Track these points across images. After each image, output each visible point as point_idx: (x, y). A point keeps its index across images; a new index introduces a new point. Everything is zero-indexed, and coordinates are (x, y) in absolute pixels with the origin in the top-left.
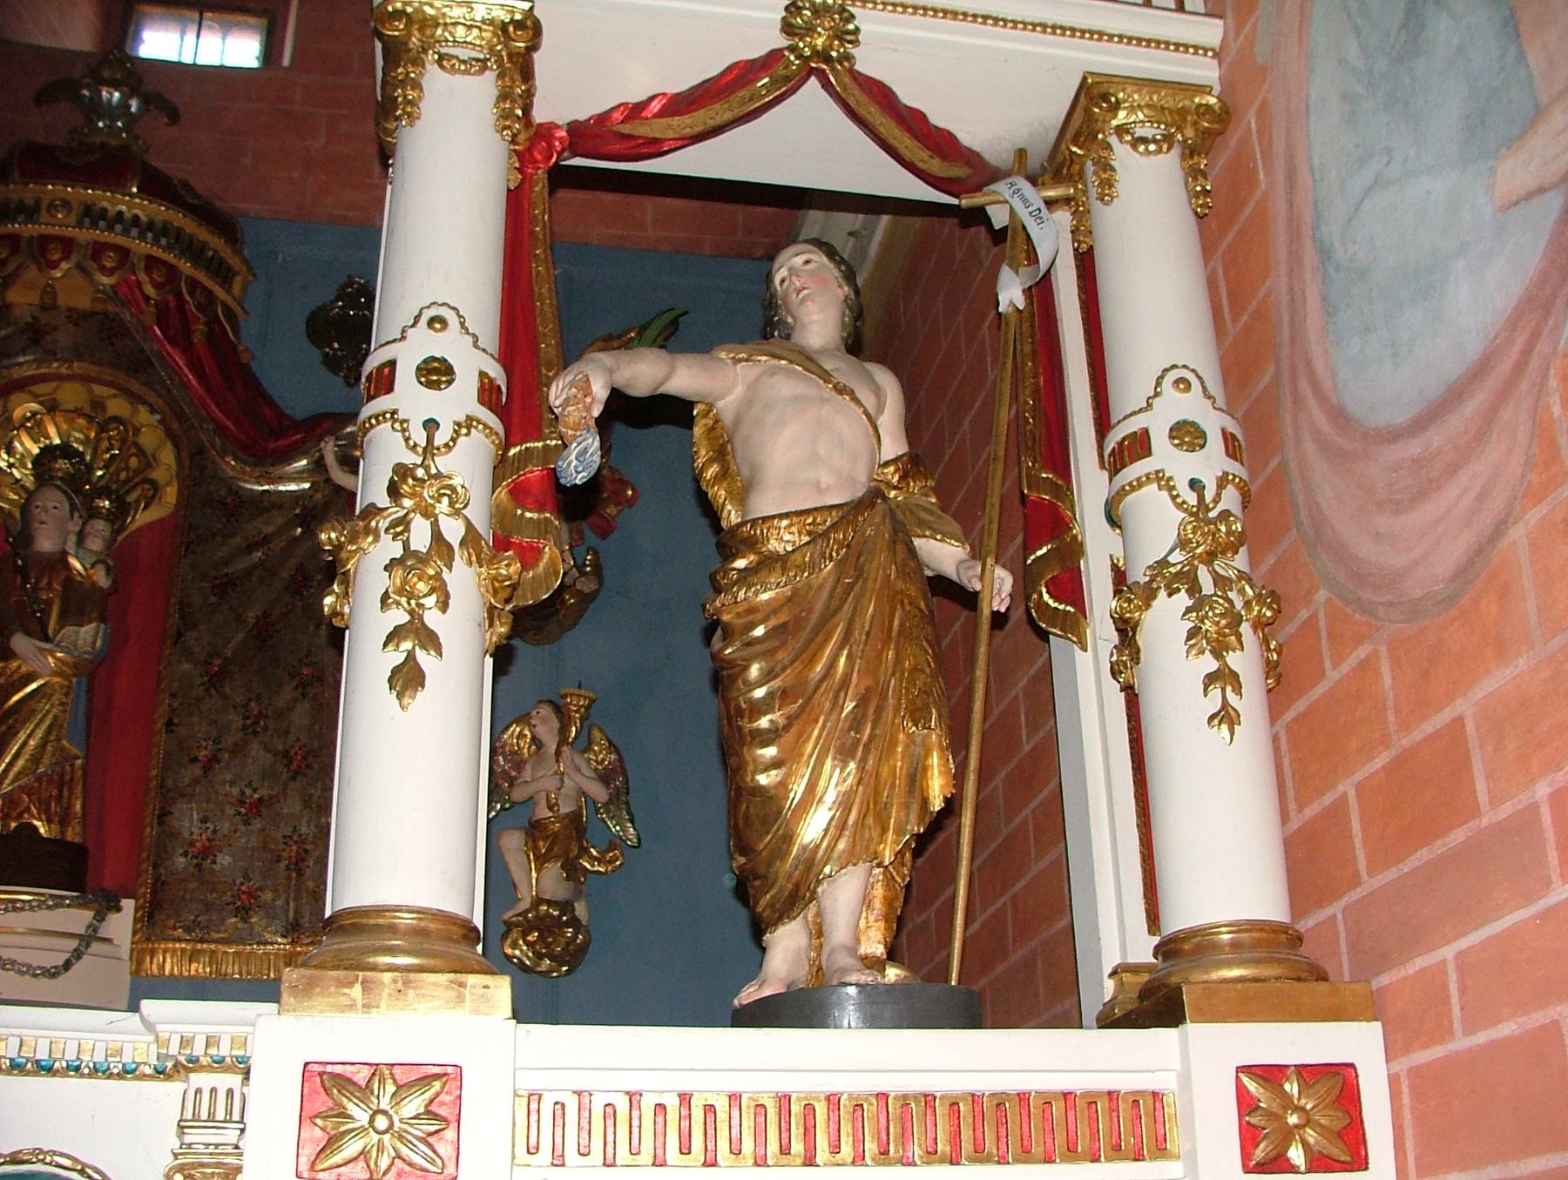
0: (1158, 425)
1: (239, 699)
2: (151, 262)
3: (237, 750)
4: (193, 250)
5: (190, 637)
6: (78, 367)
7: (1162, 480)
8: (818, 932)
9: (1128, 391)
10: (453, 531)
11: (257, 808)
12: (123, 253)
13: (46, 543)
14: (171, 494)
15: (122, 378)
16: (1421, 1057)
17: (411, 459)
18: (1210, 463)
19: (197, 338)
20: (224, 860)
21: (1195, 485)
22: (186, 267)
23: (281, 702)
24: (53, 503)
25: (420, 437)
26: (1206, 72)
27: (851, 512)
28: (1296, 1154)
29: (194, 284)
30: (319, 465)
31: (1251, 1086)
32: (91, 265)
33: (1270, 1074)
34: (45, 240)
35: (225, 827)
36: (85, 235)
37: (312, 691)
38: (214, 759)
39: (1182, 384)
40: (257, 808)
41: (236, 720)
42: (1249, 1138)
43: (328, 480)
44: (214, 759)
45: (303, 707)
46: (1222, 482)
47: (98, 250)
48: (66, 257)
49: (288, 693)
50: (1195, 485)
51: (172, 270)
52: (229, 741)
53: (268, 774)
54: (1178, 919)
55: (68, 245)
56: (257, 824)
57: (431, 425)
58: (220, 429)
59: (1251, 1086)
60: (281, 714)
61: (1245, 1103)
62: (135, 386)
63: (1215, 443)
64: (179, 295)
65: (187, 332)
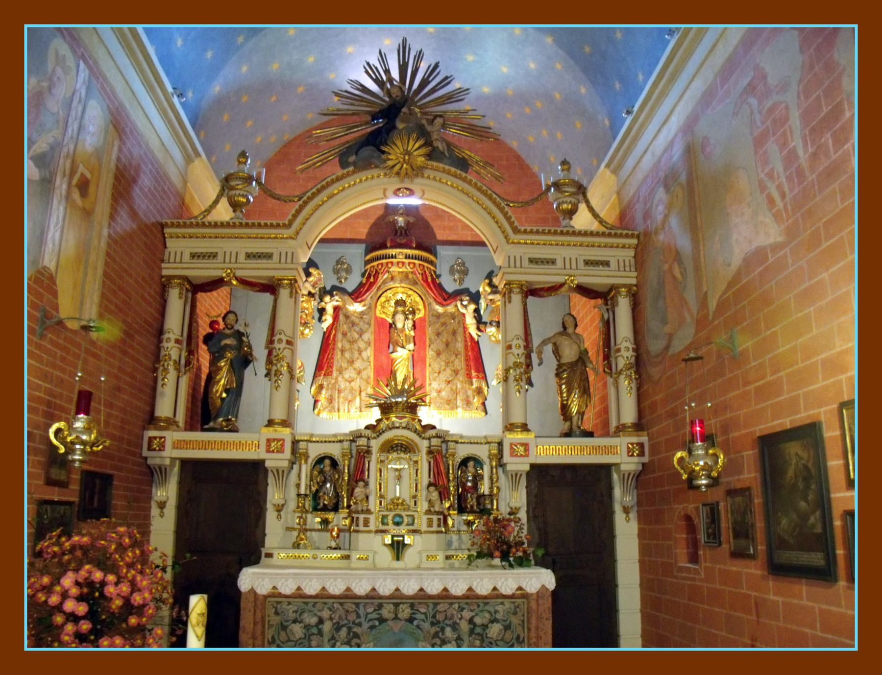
0: (622, 347)
1: (444, 359)
2: (420, 265)
3: (444, 370)
4: (426, 260)
5: (432, 346)
6: (403, 285)
7: (622, 356)
8: (571, 423)
9: (619, 341)
10: (522, 370)
11: (449, 382)
12: (414, 264)
13: (399, 325)
14: (423, 312)
15: (412, 287)
16: (652, 442)
17: (515, 360)
18: (630, 353)
19: (430, 280)
20: (443, 393)
21: (627, 357)
22: (426, 264)
23: (452, 359)
24: (400, 318)
25: (516, 356)
26: (634, 281)
27: (577, 361)
28: (635, 454)
29: (428, 268)
30: (456, 306)
31: (630, 446)
32: (408, 267)
33: (632, 444)
34: (398, 263)
35: (443, 387)
36: (407, 261)
37: (459, 356)
38: (439, 373)
39: (626, 341)
40: (449, 382)
41: (443, 363)
42: (629, 452)
43: (458, 309)
44: (439, 373)
45: (457, 360)
46: (632, 356)
47: (409, 263)
48: (403, 265)
49: (454, 357)
50: (627, 357)
51: (424, 266)
52: (442, 368)
53: (451, 375)
54: (623, 421)
55: (403, 263)
56: (450, 385)
57: (518, 355)
58: (435, 300)
59: (630, 446)
60: (452, 362)
61: (628, 448)
62: (414, 289)
63: (631, 350)
64: (425, 272)
65: (427, 279)
